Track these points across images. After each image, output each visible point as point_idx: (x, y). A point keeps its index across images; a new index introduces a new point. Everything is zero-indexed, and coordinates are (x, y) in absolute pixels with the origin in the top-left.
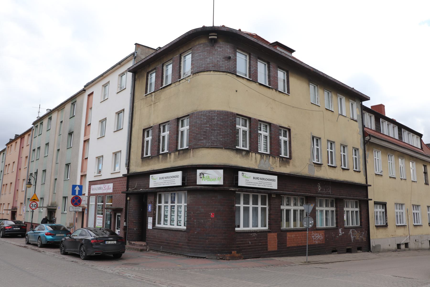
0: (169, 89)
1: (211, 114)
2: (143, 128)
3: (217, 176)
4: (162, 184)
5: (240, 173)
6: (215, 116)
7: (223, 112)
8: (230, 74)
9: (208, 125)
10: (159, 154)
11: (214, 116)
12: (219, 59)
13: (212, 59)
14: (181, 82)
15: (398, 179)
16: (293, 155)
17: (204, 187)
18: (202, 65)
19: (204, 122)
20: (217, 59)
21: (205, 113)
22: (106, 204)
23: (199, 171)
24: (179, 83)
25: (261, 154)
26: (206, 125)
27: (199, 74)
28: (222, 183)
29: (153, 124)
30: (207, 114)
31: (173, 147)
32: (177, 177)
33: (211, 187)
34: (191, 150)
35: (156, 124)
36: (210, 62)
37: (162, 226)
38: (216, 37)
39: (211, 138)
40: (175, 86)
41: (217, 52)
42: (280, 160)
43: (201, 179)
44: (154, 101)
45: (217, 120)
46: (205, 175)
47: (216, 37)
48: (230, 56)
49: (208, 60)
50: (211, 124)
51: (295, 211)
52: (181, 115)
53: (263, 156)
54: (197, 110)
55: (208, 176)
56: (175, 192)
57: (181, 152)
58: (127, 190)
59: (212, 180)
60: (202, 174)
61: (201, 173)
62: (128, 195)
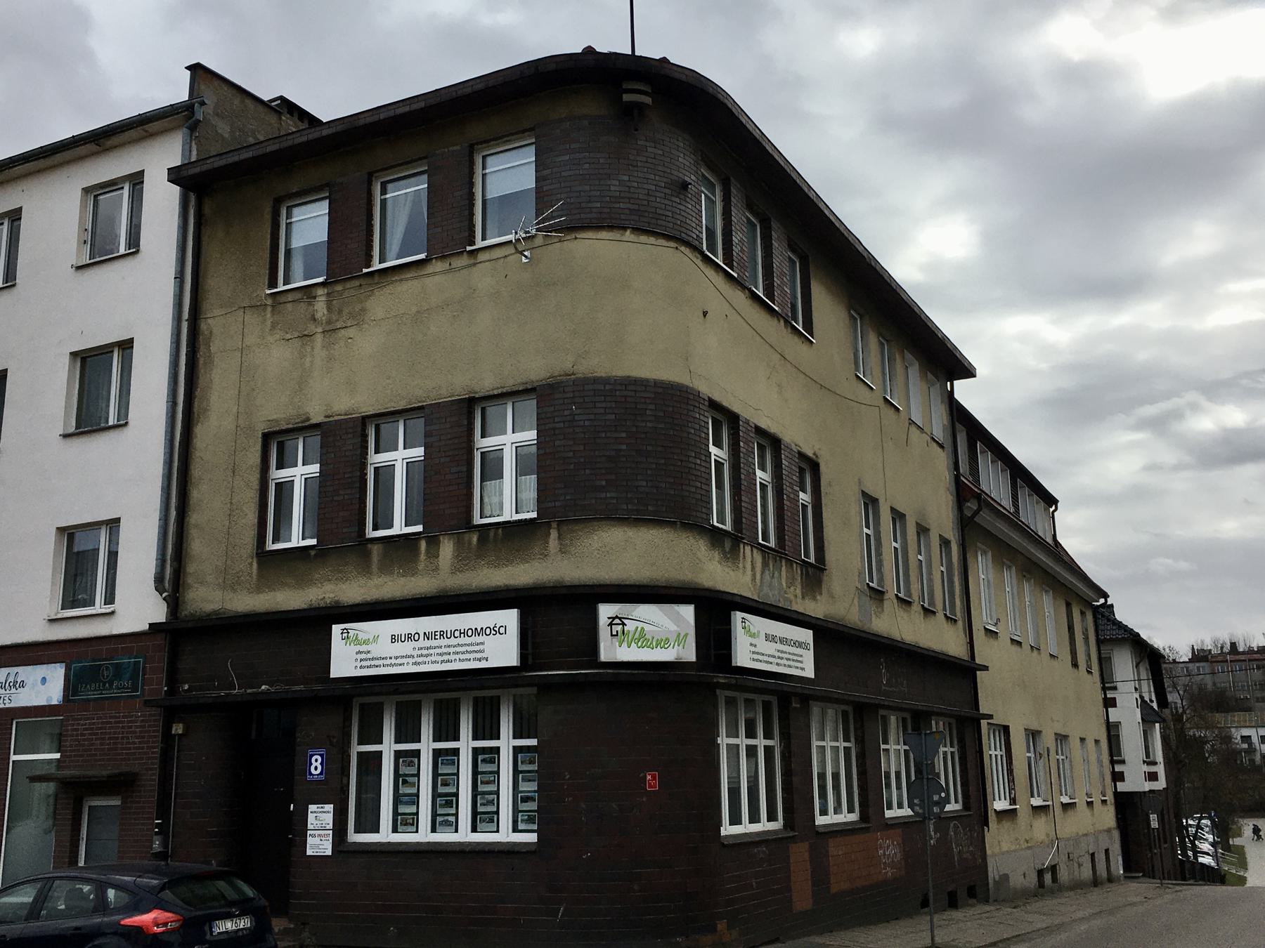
0: (415, 278)
1: (633, 394)
2: (261, 428)
3: (673, 627)
4: (411, 660)
5: (738, 616)
6: (645, 402)
7: (673, 389)
8: (688, 249)
9: (624, 435)
10: (364, 543)
11: (643, 400)
12: (653, 188)
13: (628, 184)
14: (482, 257)
16: (831, 555)
17: (629, 672)
18: (590, 202)
19: (608, 423)
20: (645, 186)
21: (608, 387)
22: (14, 758)
23: (606, 611)
24: (472, 261)
25: (763, 549)
26: (617, 435)
27: (577, 236)
28: (690, 655)
29: (329, 413)
30: (618, 393)
31: (446, 512)
32: (496, 631)
33: (643, 672)
34: (550, 527)
35: (339, 417)
36: (622, 195)
37: (385, 835)
38: (648, 100)
39: (636, 484)
40: (450, 270)
41: (644, 159)
42: (802, 571)
43: (615, 639)
44: (329, 322)
45: (655, 416)
46: (630, 626)
47: (648, 100)
48: (687, 179)
49: (615, 187)
50: (634, 429)
51: (996, 755)
52: (487, 383)
53: (778, 558)
54: (575, 375)
55: (639, 629)
56: (461, 693)
57: (496, 534)
58: (173, 691)
59: (654, 644)
60: (617, 621)
61: (613, 619)
62: (171, 713)
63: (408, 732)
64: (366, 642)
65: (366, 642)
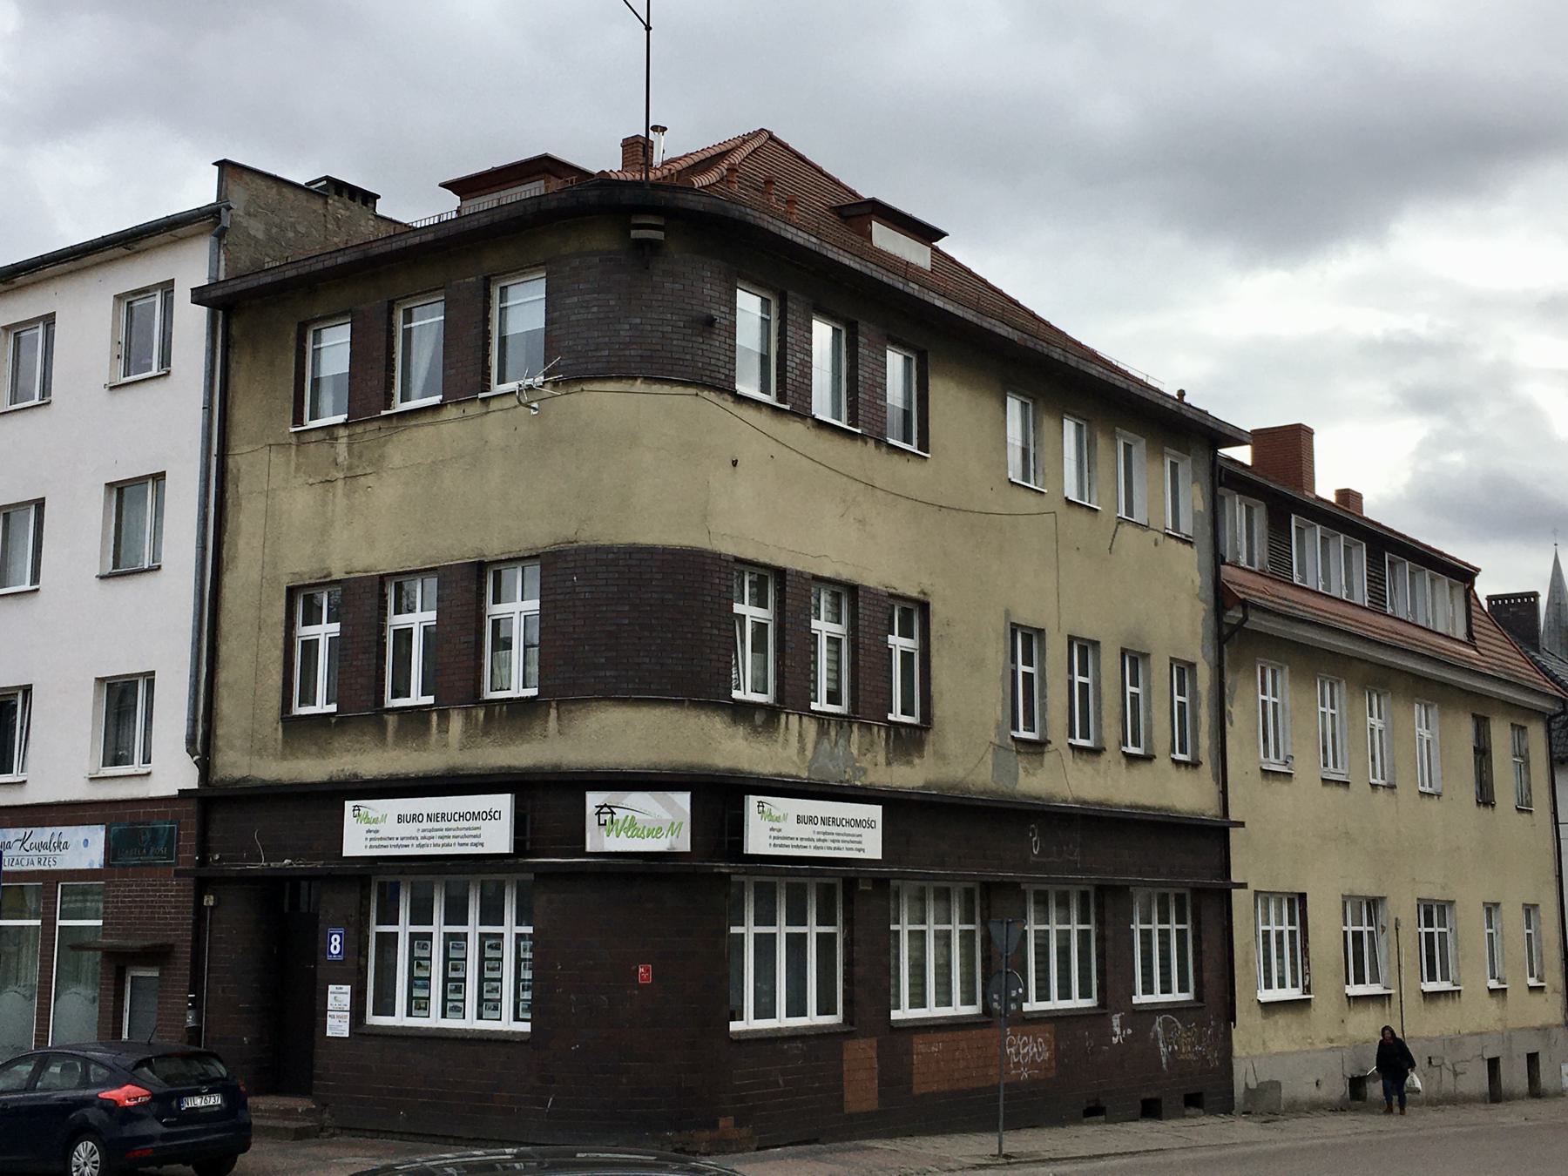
2: (286, 581)
3: (666, 816)
4: (415, 842)
5: (752, 801)
8: (712, 393)
9: (627, 608)
10: (380, 711)
14: (494, 405)
15: (1359, 787)
16: (940, 710)
18: (596, 350)
21: (611, 556)
22: (60, 923)
23: (593, 799)
25: (821, 717)
27: (585, 388)
28: (684, 845)
29: (349, 569)
32: (492, 815)
34: (550, 706)
37: (400, 1019)
40: (464, 418)
42: (888, 736)
43: (603, 828)
44: (350, 468)
46: (620, 814)
49: (624, 330)
52: (494, 548)
54: (577, 542)
55: (630, 818)
58: (203, 861)
59: (645, 833)
60: (605, 810)
61: (602, 807)
62: (203, 885)
63: (421, 914)
64: (375, 821)
65: (375, 821)
